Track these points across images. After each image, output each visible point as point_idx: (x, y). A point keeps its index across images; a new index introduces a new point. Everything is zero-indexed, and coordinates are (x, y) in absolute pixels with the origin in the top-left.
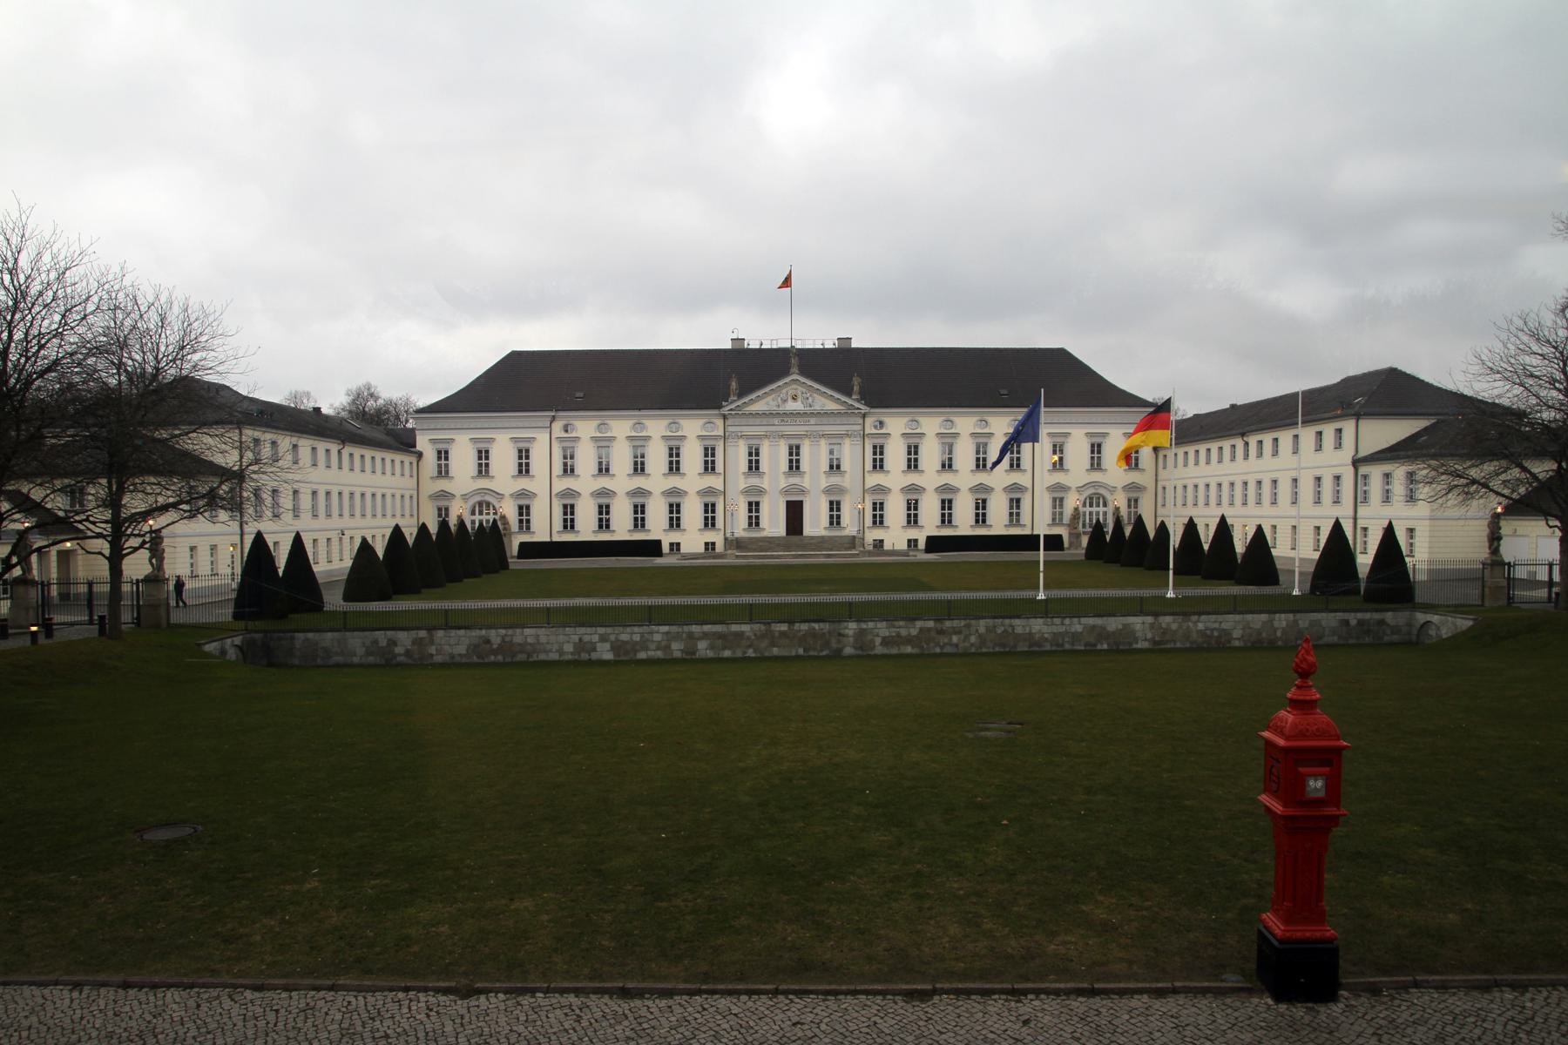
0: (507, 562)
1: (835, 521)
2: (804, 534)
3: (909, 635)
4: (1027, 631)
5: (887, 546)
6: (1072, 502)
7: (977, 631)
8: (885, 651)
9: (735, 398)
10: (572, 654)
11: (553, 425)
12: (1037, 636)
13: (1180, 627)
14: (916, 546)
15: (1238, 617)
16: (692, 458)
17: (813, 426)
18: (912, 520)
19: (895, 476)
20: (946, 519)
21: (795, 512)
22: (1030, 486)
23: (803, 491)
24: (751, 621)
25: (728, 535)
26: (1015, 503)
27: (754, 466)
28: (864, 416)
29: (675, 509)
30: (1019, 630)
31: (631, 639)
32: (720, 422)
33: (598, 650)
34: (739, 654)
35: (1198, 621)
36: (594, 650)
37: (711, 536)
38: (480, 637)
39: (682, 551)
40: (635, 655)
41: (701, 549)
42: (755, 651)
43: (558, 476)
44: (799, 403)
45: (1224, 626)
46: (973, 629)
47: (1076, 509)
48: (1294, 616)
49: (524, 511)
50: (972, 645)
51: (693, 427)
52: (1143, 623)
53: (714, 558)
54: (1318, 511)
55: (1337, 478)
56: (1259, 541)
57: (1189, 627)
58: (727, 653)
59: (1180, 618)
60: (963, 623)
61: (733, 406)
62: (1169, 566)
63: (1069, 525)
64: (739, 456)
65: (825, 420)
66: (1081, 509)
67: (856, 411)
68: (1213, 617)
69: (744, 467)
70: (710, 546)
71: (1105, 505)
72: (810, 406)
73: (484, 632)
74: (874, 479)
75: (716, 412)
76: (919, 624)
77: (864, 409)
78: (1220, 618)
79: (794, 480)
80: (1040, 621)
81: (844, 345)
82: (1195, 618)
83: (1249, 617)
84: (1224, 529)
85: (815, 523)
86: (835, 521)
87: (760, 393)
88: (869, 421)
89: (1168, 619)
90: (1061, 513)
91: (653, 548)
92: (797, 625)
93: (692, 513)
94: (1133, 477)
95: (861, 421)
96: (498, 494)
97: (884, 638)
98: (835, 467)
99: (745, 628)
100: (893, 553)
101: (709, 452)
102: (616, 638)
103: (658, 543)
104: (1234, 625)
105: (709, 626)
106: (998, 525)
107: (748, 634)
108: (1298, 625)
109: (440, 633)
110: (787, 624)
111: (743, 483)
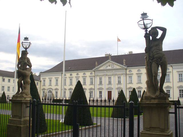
17: (114, 72)
21: (110, 93)
22: (172, 86)
27: (101, 83)
28: (126, 69)
32: (93, 73)
49: (57, 93)
64: (97, 80)
65: (117, 71)
77: (126, 68)
79: (110, 86)
87: (101, 65)
88: (128, 71)
95: (125, 70)
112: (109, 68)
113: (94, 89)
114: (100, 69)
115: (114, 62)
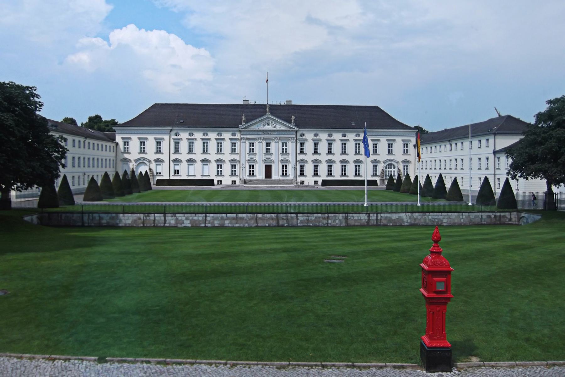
0: (151, 187)
1: (284, 173)
2: (272, 178)
3: (311, 219)
4: (359, 219)
5: (306, 183)
6: (380, 167)
7: (339, 218)
8: (301, 225)
9: (244, 124)
10: (174, 224)
11: (171, 133)
12: (363, 220)
13: (422, 218)
14: (317, 183)
15: (445, 214)
16: (227, 146)
18: (316, 173)
19: (309, 156)
20: (330, 173)
21: (268, 170)
23: (272, 161)
24: (246, 213)
25: (241, 178)
26: (357, 167)
27: (252, 151)
28: (296, 132)
29: (219, 166)
30: (356, 218)
31: (198, 218)
33: (185, 223)
34: (242, 225)
35: (429, 215)
36: (183, 223)
37: (234, 178)
38: (137, 217)
39: (222, 184)
40: (200, 225)
41: (231, 183)
42: (248, 225)
43: (173, 153)
44: (270, 126)
45: (440, 217)
46: (337, 218)
47: (382, 170)
48: (468, 214)
50: (337, 224)
51: (227, 135)
52: (407, 216)
53: (236, 186)
54: (480, 172)
55: (487, 159)
56: (455, 183)
57: (425, 217)
58: (237, 225)
59: (421, 214)
60: (333, 215)
61: (243, 127)
62: (418, 193)
63: (379, 176)
64: (246, 146)
66: (385, 170)
67: (293, 130)
68: (435, 214)
69: (248, 151)
70: (234, 182)
71: (394, 168)
72: (275, 128)
73: (138, 215)
74: (300, 157)
75: (237, 129)
76: (315, 215)
77: (296, 129)
78: (438, 214)
80: (364, 215)
81: (288, 103)
82: (427, 214)
83: (450, 214)
84: (441, 180)
85: (276, 173)
86: (284, 173)
87: (254, 122)
88: (298, 134)
89: (417, 214)
90: (376, 171)
91: (211, 182)
92: (266, 214)
93: (227, 168)
94: (406, 157)
95: (294, 133)
96: (148, 160)
97: (301, 221)
98: (284, 151)
99: (244, 215)
100: (308, 186)
101: (234, 144)
102: (192, 218)
103: (213, 181)
104: (445, 218)
105: (230, 214)
106: (351, 175)
107: (245, 218)
108: (470, 217)
109: (121, 215)
110: (261, 214)
111: (248, 157)
112: (267, 127)
113: (240, 162)
114: (249, 128)
115: (277, 119)
